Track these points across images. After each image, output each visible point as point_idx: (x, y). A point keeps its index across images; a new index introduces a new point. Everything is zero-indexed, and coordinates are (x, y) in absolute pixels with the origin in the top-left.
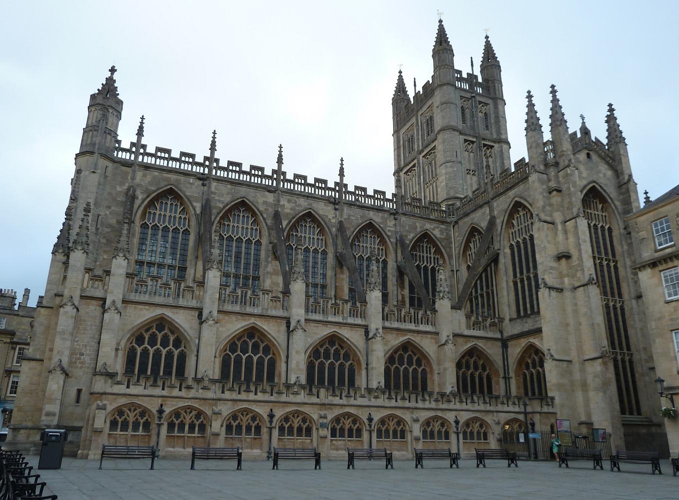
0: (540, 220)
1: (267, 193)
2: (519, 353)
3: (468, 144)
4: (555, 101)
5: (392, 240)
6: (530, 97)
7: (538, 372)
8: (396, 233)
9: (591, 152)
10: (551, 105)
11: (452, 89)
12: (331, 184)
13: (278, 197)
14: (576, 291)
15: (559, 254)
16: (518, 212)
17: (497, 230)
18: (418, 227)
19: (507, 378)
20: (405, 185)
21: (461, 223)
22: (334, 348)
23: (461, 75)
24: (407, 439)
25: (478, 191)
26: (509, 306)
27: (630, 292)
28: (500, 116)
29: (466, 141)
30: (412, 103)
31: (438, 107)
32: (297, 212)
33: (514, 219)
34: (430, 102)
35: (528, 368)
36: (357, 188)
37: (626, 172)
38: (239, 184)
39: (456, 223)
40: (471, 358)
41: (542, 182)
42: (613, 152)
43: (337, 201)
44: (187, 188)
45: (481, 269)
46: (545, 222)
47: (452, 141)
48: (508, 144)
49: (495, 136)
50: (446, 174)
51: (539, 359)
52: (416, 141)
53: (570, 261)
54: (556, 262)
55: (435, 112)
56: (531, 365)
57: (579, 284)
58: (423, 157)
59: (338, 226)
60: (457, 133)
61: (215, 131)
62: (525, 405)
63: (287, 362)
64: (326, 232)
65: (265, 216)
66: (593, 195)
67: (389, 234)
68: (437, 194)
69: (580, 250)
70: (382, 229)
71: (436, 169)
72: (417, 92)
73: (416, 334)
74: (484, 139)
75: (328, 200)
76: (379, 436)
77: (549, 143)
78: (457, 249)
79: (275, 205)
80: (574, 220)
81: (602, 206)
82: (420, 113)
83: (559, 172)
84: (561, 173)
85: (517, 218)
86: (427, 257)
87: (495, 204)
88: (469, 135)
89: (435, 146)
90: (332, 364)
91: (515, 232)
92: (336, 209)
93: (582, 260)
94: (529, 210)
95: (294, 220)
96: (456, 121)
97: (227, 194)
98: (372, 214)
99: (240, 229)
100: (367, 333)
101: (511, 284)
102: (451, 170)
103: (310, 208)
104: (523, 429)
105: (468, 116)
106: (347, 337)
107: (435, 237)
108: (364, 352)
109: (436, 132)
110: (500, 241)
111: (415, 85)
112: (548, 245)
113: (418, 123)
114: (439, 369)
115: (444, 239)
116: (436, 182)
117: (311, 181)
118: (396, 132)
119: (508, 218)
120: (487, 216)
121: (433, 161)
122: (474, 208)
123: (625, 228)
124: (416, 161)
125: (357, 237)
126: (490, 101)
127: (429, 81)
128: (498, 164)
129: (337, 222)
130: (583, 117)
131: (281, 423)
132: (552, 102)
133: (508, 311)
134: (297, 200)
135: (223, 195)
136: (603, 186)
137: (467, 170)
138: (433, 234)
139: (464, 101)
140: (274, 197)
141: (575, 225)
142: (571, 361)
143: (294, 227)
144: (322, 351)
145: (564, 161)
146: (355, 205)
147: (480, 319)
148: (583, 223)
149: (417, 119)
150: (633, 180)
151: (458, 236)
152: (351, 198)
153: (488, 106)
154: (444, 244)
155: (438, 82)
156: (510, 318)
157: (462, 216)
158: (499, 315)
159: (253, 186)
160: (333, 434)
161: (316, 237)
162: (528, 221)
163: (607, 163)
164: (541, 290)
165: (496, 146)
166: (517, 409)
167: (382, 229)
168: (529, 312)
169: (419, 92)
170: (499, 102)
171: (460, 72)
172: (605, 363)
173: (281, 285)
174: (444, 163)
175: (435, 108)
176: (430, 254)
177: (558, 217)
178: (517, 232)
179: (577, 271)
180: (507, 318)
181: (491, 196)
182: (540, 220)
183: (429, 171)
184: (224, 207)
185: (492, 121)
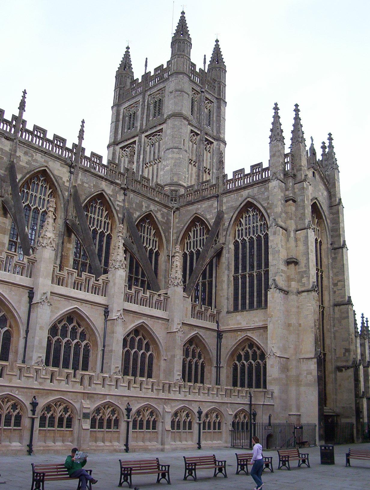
0: (277, 225)
2: (234, 345)
3: (193, 135)
4: (297, 119)
5: (119, 215)
6: (276, 109)
7: (251, 365)
8: (123, 208)
9: (315, 172)
11: (186, 79)
12: (69, 145)
13: (16, 147)
14: (299, 295)
15: (289, 259)
16: (248, 212)
18: (144, 207)
19: (218, 368)
21: (183, 210)
22: (72, 325)
23: (195, 68)
24: (158, 430)
25: (206, 184)
26: (228, 299)
27: (330, 301)
29: (192, 131)
30: (140, 81)
31: (171, 93)
34: (161, 86)
35: (239, 358)
36: (93, 154)
37: (338, 196)
39: (178, 209)
40: (191, 345)
42: (329, 175)
43: (74, 164)
45: (208, 260)
46: (281, 227)
47: (181, 128)
49: (215, 134)
50: (172, 158)
51: (253, 352)
52: (139, 119)
53: (297, 266)
54: (286, 266)
55: (166, 96)
56: (243, 357)
57: (303, 289)
58: (146, 136)
60: (187, 123)
63: (26, 338)
64: (59, 196)
66: (315, 208)
67: (118, 208)
68: (157, 176)
69: (308, 259)
70: (112, 202)
71: (159, 151)
72: (147, 72)
73: (149, 319)
74: (206, 134)
75: (65, 162)
76: (134, 427)
77: (290, 155)
80: (305, 230)
81: (318, 221)
82: (149, 93)
83: (295, 184)
85: (246, 217)
86: (147, 238)
87: (225, 200)
88: (196, 127)
89: (162, 129)
90: (68, 343)
91: (242, 230)
92: (71, 172)
93: (309, 268)
94: (260, 211)
95: (28, 176)
96: (186, 111)
98: (104, 185)
100: (106, 313)
101: (232, 279)
102: (177, 156)
103: (46, 166)
104: (247, 419)
105: (196, 108)
106: (87, 315)
107: (157, 219)
108: (102, 333)
109: (165, 116)
110: (226, 236)
111: (146, 65)
112: (281, 250)
113: (144, 102)
114: (167, 355)
116: (158, 164)
117: (50, 136)
118: (117, 105)
119: (237, 215)
120: (215, 209)
121: (157, 144)
122: (200, 199)
123: (331, 244)
124: (136, 139)
125: (86, 207)
126: (215, 100)
127: (163, 65)
128: (214, 160)
129: (71, 186)
131: (43, 412)
133: (226, 304)
134: (34, 154)
136: (320, 203)
137: (190, 160)
138: (156, 216)
139: (194, 93)
140: (11, 146)
142: (289, 358)
143: (27, 183)
144: (60, 326)
145: (301, 175)
147: (203, 309)
148: (312, 236)
149: (144, 98)
150: (342, 204)
151: (178, 223)
152: (86, 164)
153: (212, 104)
154: (163, 228)
155: (173, 68)
156: (227, 311)
157: (185, 203)
158: (215, 307)
160: (93, 426)
161: (47, 199)
163: (325, 185)
165: (215, 143)
167: (112, 202)
168: (247, 307)
169: (150, 72)
170: (222, 103)
171: (194, 65)
173: (7, 246)
174: (171, 148)
175: (167, 93)
176: (150, 236)
177: (292, 225)
178: (244, 230)
179: (303, 277)
180: (225, 310)
181: (221, 191)
182: (277, 225)
185: (214, 119)
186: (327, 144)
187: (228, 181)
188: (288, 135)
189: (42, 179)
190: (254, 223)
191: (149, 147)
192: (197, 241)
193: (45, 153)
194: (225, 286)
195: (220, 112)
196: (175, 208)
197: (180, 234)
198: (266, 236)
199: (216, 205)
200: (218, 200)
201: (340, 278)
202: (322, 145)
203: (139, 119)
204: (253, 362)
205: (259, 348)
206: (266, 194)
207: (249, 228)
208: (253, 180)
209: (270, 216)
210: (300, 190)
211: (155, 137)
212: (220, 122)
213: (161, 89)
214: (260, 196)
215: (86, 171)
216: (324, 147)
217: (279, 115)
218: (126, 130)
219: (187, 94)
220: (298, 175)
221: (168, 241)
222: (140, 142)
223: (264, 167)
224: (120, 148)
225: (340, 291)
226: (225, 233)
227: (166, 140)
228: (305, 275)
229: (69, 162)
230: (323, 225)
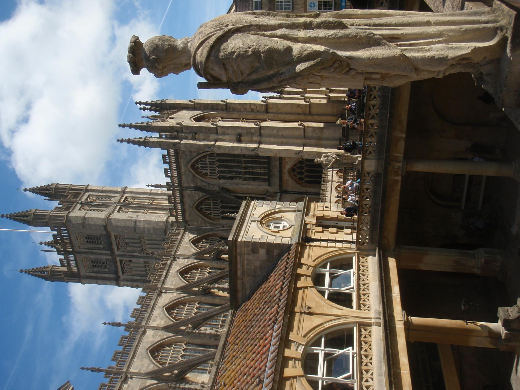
3: (121, 211)
4: (131, 126)
6: (122, 141)
7: (307, 171)
10: (133, 129)
16: (198, 168)
17: (205, 186)
18: (186, 245)
20: (134, 275)
21: (188, 218)
26: (260, 185)
28: (102, 189)
29: (118, 211)
30: (62, 257)
32: (165, 316)
43: (159, 290)
48: (126, 188)
52: (99, 257)
53: (242, 135)
58: (118, 251)
59: (180, 291)
60: (112, 215)
65: (165, 337)
67: (190, 263)
68: (155, 240)
71: (134, 239)
83: (183, 132)
84: (184, 131)
85: (201, 169)
88: (115, 209)
89: (115, 235)
92: (166, 292)
94: (199, 158)
97: (142, 361)
101: (245, 182)
109: (104, 232)
110: (214, 185)
113: (85, 253)
123: (223, 110)
124: (118, 259)
126: (87, 194)
134: (154, 315)
135: (142, 364)
136: (193, 115)
139: (83, 209)
146: (164, 280)
158: (265, 195)
162: (206, 161)
164: (258, 153)
170: (89, 188)
179: (250, 132)
180: (267, 188)
183: (133, 247)
184: (154, 363)
186: (142, 106)
190: (207, 164)
194: (250, 187)
196: (186, 225)
197: (207, 221)
198: (218, 155)
199: (190, 191)
200: (185, 190)
201: (248, 107)
203: (99, 257)
204: (305, 169)
206: (187, 153)
208: (174, 163)
209: (205, 151)
211: (120, 242)
213: (77, 237)
216: (144, 109)
218: (107, 270)
219: (86, 213)
221: (212, 230)
222: (122, 256)
223: (167, 154)
224: (123, 274)
226: (211, 186)
227: (126, 232)
228: (249, 130)
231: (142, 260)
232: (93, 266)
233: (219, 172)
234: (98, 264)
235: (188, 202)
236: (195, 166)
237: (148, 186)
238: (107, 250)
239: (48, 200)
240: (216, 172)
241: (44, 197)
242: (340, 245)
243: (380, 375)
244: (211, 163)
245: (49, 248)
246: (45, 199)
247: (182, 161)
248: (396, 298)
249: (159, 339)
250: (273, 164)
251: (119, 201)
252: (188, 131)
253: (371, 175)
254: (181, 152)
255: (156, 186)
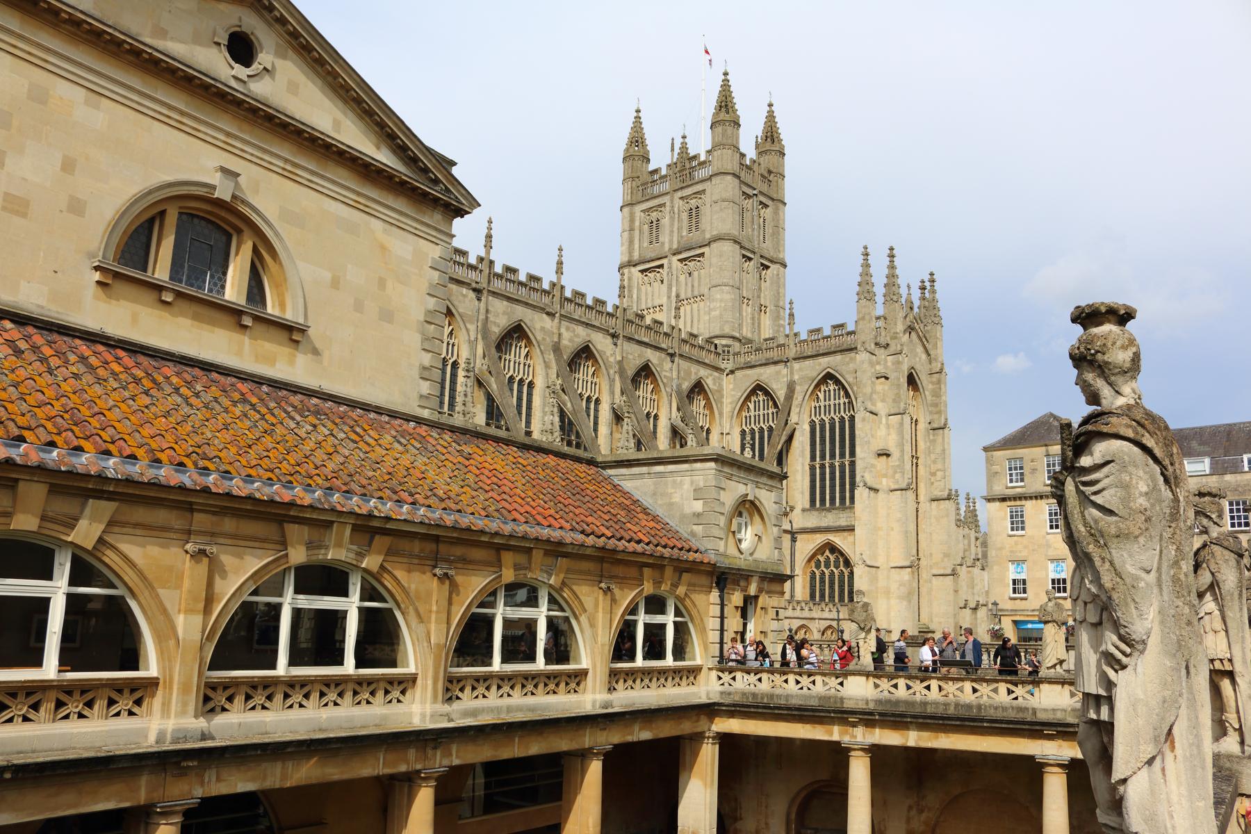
1: (544, 315)
4: (892, 267)
7: (832, 573)
10: (886, 271)
17: (797, 399)
18: (693, 374)
20: (639, 289)
21: (739, 374)
26: (802, 493)
29: (744, 256)
33: (820, 391)
34: (699, 187)
35: (818, 566)
37: (940, 359)
38: (517, 300)
39: (732, 372)
41: (872, 364)
44: (460, 302)
46: (871, 413)
48: (785, 266)
49: (772, 254)
50: (721, 301)
56: (823, 564)
57: (896, 487)
61: (490, 219)
62: (838, 612)
64: (603, 375)
66: (912, 381)
67: (665, 381)
68: (699, 321)
69: (902, 451)
71: (699, 285)
78: (729, 406)
79: (553, 334)
82: (679, 194)
85: (825, 391)
92: (615, 344)
94: (844, 388)
99: (512, 363)
101: (807, 468)
102: (727, 297)
109: (708, 236)
115: (717, 391)
120: (783, 377)
122: (764, 362)
124: (664, 261)
126: (769, 202)
130: (909, 286)
132: (888, 267)
134: (575, 327)
135: (498, 316)
141: (900, 421)
145: (896, 345)
148: (907, 419)
149: (672, 201)
151: (733, 390)
153: (768, 209)
157: (742, 365)
159: (531, 305)
162: (839, 399)
165: (773, 266)
166: (831, 617)
168: (828, 505)
171: (743, 155)
172: (913, 572)
175: (707, 198)
179: (895, 472)
186: (927, 284)
187: (800, 342)
188: (879, 290)
189: (584, 356)
190: (835, 399)
191: (684, 276)
192: (759, 415)
193: (587, 325)
194: (799, 477)
195: (778, 220)
198: (852, 418)
201: (939, 466)
202: (920, 284)
203: (667, 232)
204: (834, 570)
205: (842, 554)
206: (851, 365)
207: (830, 406)
210: (893, 364)
211: (693, 262)
212: (779, 234)
214: (844, 367)
215: (630, 338)
216: (923, 288)
217: (869, 262)
220: (892, 344)
225: (938, 483)
229: (612, 331)
230: (920, 400)
231: (664, 300)
232: (652, 222)
233: (822, 422)
234: (654, 230)
235: (768, 372)
236: (831, 380)
237: (791, 303)
238: (679, 242)
239: (757, 142)
240: (823, 416)
241: (760, 134)
242: (714, 636)
243: (509, 709)
244: (837, 408)
245: (677, 150)
246: (757, 137)
247: (838, 357)
248: (632, 734)
249: (538, 338)
250: (841, 515)
251: (761, 256)
252: (889, 364)
253: (839, 687)
254: (852, 354)
255: (792, 315)
